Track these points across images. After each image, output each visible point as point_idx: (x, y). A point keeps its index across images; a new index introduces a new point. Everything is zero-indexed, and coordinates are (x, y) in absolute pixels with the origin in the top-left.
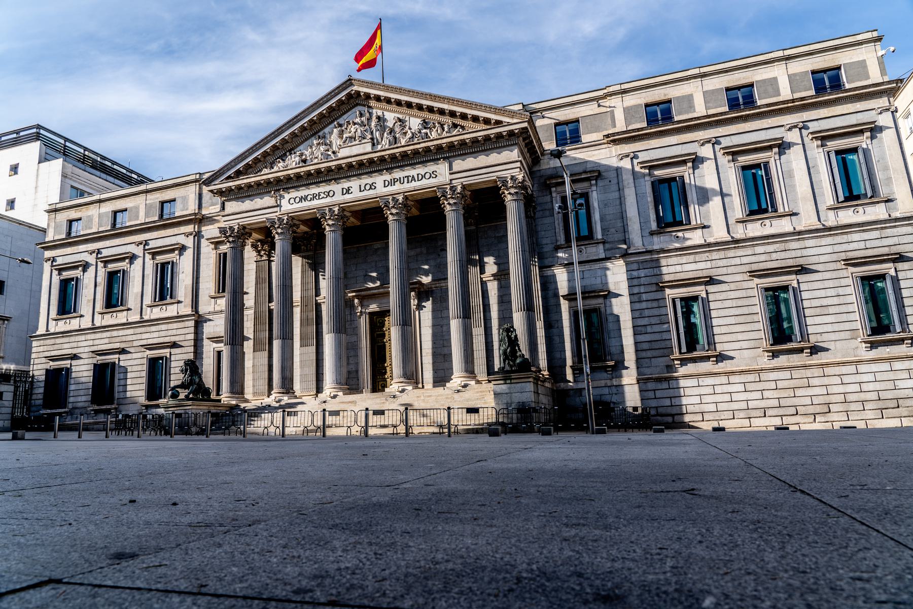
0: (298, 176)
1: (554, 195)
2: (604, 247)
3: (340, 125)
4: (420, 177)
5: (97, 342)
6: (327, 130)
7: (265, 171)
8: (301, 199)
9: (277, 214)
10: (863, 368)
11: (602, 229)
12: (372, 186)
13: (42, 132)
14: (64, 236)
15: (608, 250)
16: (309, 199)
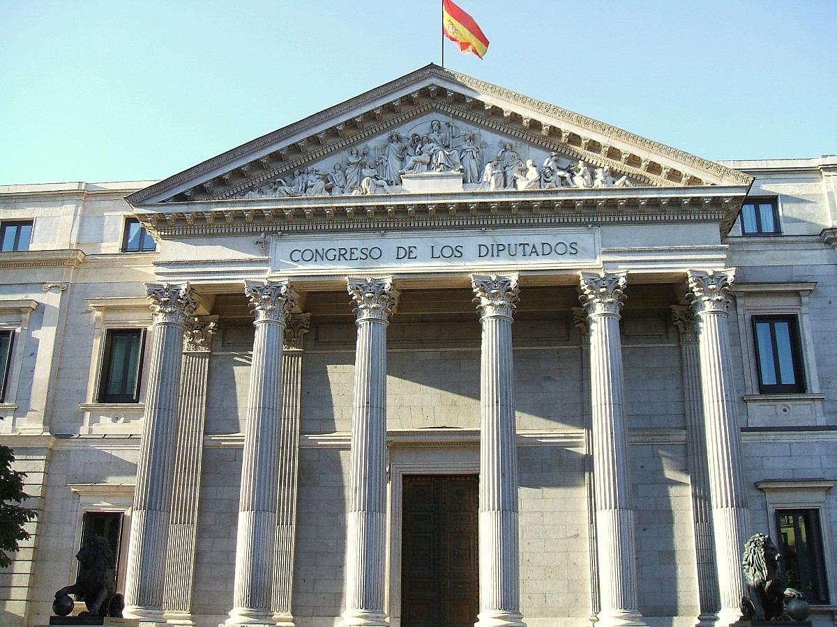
0: (319, 212)
1: (740, 311)
2: (823, 407)
3: (399, 139)
4: (547, 249)
6: (372, 144)
7: (255, 195)
8: (319, 256)
9: (267, 275)
11: (820, 378)
12: (457, 253)
15: (830, 413)
16: (331, 255)
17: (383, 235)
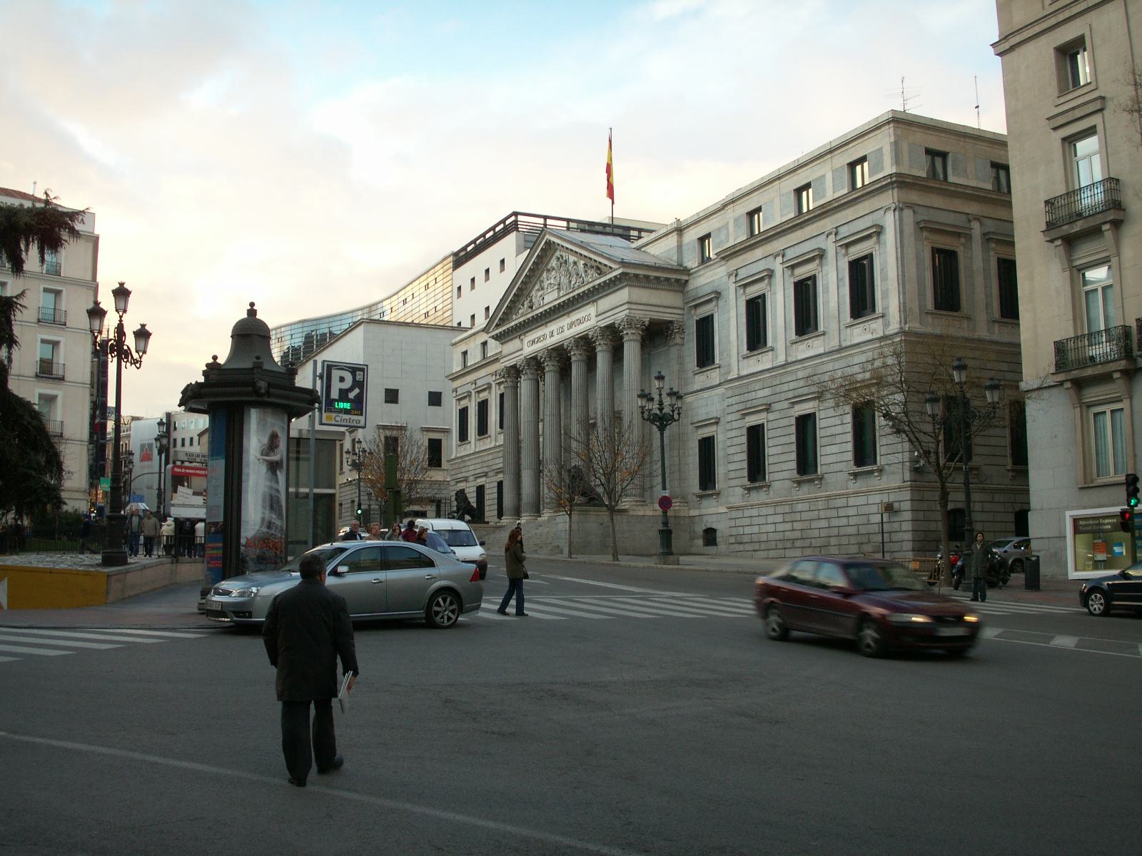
5: (477, 466)
8: (533, 342)
9: (523, 356)
10: (852, 501)
13: (520, 218)
14: (460, 368)
17: (546, 327)
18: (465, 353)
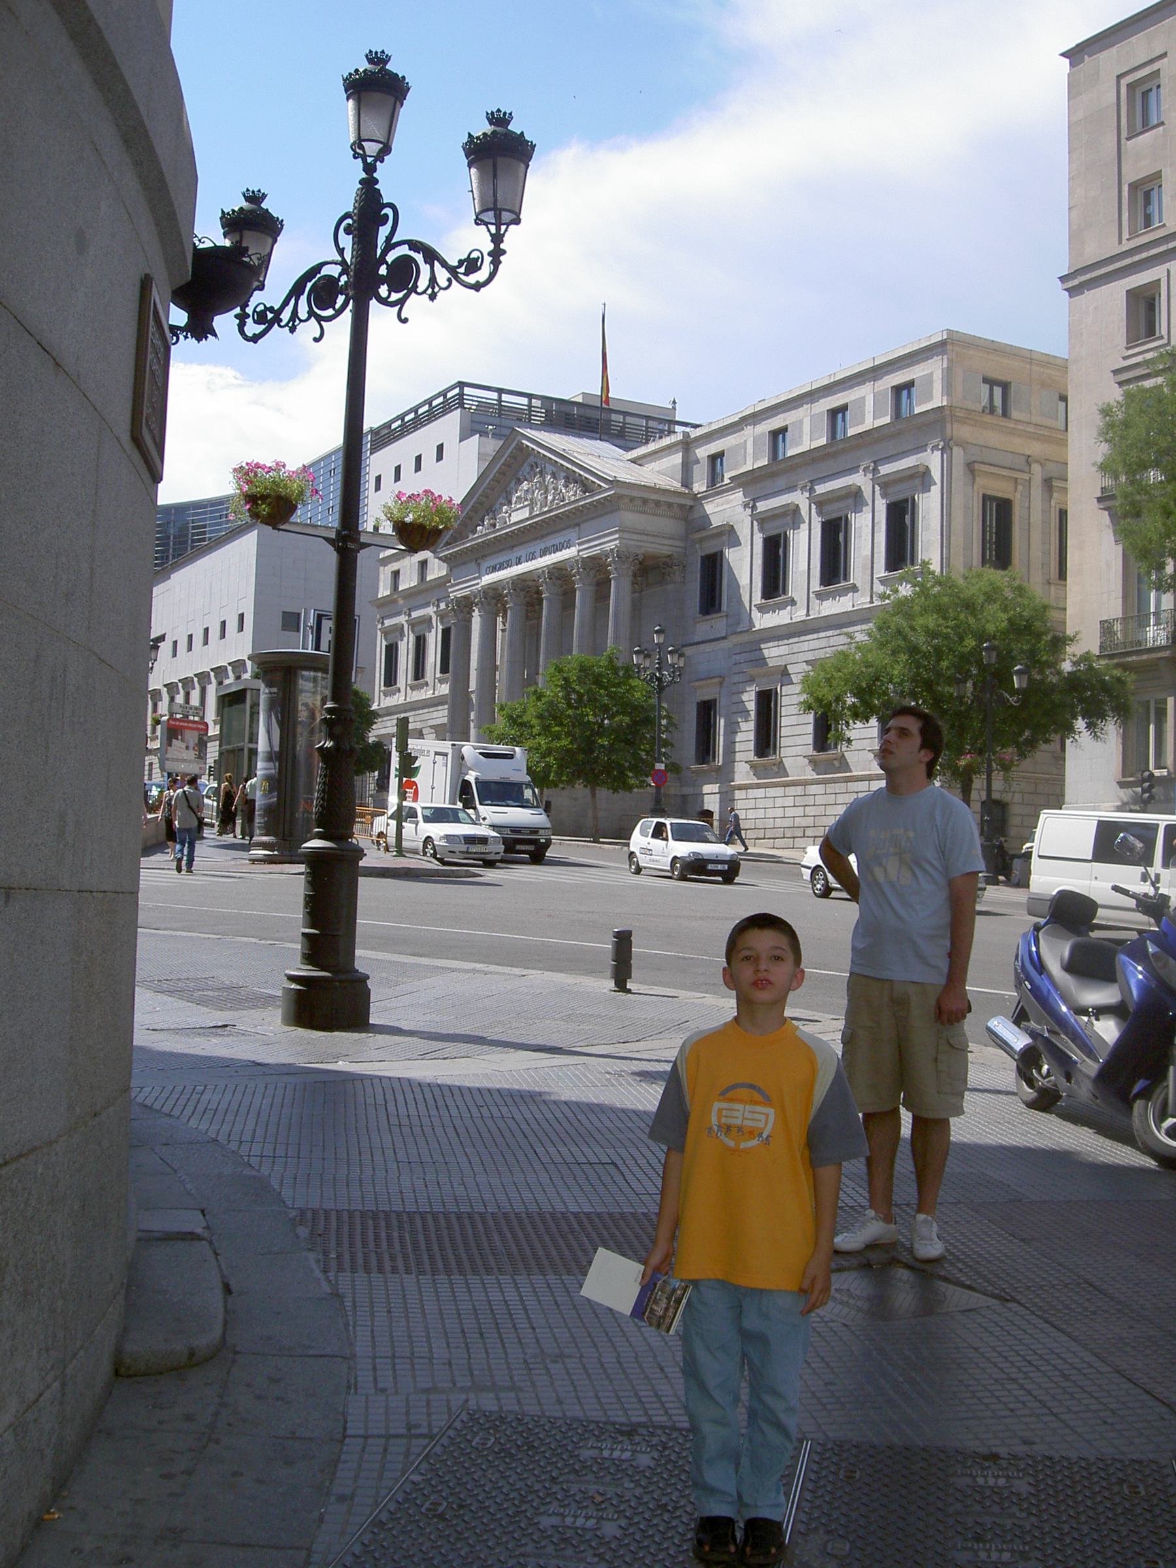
18: (396, 574)
